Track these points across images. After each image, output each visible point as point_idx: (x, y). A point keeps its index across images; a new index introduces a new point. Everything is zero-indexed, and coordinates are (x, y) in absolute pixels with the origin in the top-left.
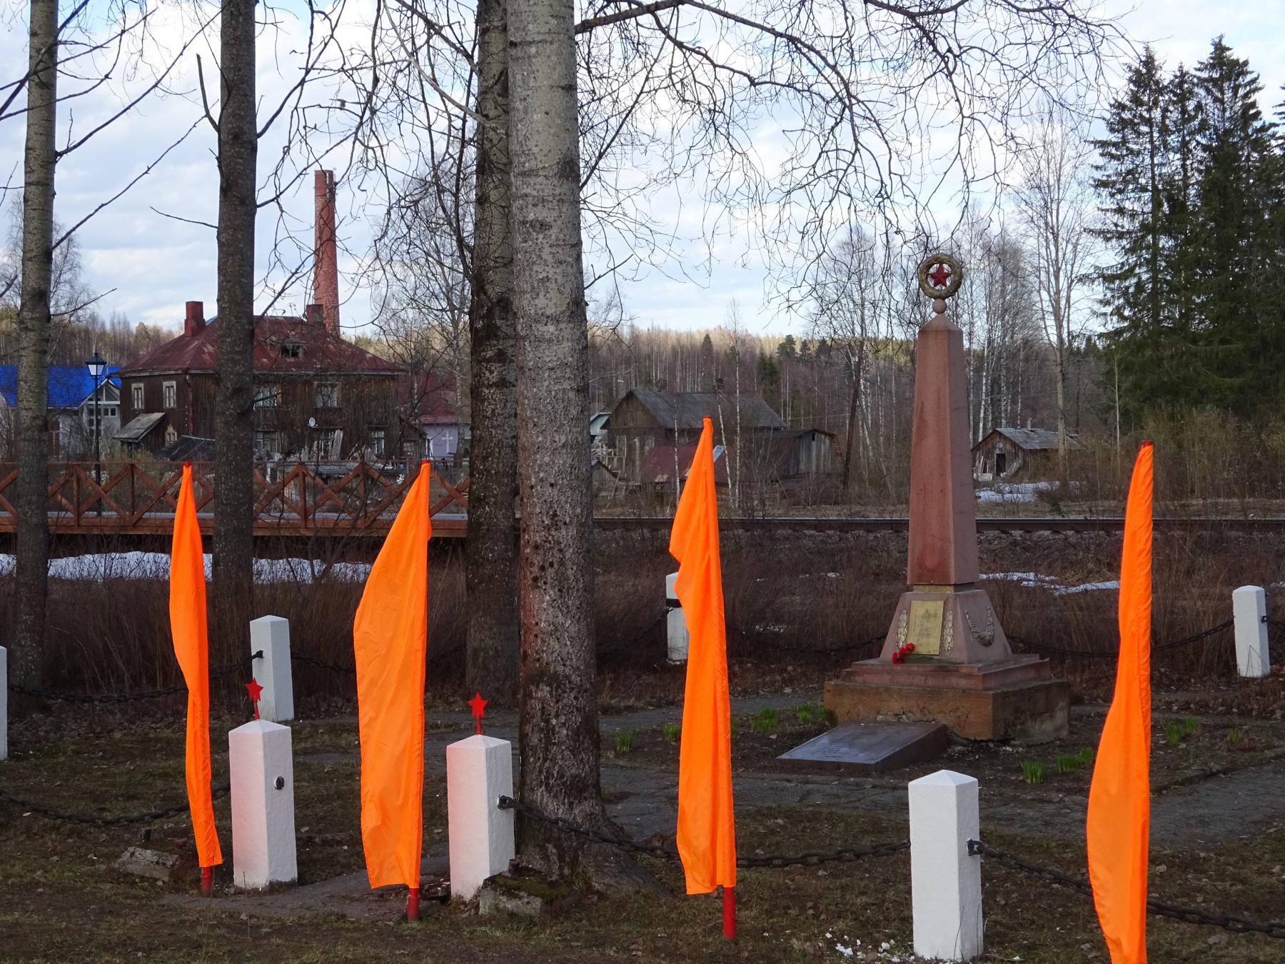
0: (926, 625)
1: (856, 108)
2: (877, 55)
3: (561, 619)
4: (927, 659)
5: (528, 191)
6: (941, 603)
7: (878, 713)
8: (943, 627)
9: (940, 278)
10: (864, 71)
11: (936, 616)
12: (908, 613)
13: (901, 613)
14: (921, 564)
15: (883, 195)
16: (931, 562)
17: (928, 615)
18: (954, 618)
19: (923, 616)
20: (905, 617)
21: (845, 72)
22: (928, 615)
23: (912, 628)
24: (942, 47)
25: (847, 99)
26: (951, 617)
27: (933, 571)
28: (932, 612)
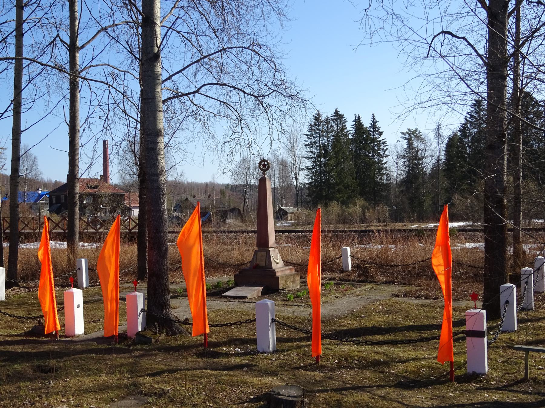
1: (242, 121)
2: (247, 107)
3: (159, 259)
4: (262, 267)
5: (149, 139)
10: (244, 112)
15: (249, 145)
17: (262, 256)
21: (239, 112)
22: (262, 256)
24: (265, 105)
25: (240, 119)
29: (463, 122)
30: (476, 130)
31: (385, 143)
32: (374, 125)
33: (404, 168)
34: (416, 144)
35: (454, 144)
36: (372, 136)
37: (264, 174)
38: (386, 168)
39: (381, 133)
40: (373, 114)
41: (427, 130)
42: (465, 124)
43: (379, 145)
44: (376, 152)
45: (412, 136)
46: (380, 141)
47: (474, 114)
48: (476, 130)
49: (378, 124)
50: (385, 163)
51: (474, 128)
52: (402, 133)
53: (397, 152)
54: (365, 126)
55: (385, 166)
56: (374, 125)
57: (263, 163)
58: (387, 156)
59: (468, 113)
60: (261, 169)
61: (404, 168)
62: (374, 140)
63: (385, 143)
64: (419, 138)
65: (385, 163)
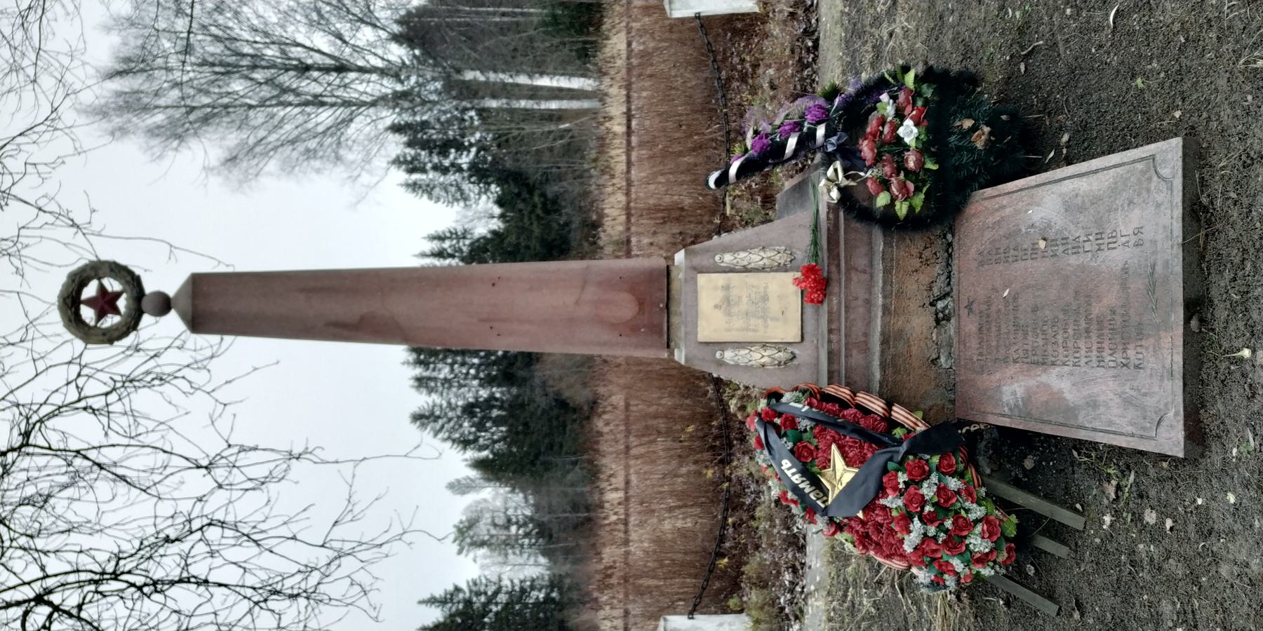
0: (744, 305)
6: (702, 279)
7: (934, 362)
8: (746, 270)
9: (105, 303)
11: (727, 288)
12: (723, 345)
13: (721, 363)
14: (631, 328)
16: (625, 308)
17: (727, 303)
18: (726, 249)
19: (729, 314)
20: (729, 355)
23: (749, 337)
26: (728, 258)
27: (641, 303)
28: (720, 294)
29: (449, 444)
30: (466, 424)
31: (475, 584)
32: (442, 602)
33: (526, 556)
34: (483, 530)
35: (491, 469)
36: (461, 606)
37: (164, 305)
38: (521, 582)
39: (458, 590)
40: (421, 602)
41: (458, 508)
42: (454, 441)
43: (478, 594)
44: (491, 600)
45: (467, 535)
46: (471, 591)
47: (438, 425)
48: (466, 424)
49: (439, 593)
50: (512, 581)
51: (461, 426)
52: (460, 552)
53: (494, 564)
54: (441, 620)
55: (516, 582)
56: (442, 602)
57: (88, 314)
58: (500, 580)
59: (436, 435)
60: (131, 324)
61: (526, 556)
62: (468, 603)
63: (475, 584)
64: (472, 523)
65: (512, 581)
